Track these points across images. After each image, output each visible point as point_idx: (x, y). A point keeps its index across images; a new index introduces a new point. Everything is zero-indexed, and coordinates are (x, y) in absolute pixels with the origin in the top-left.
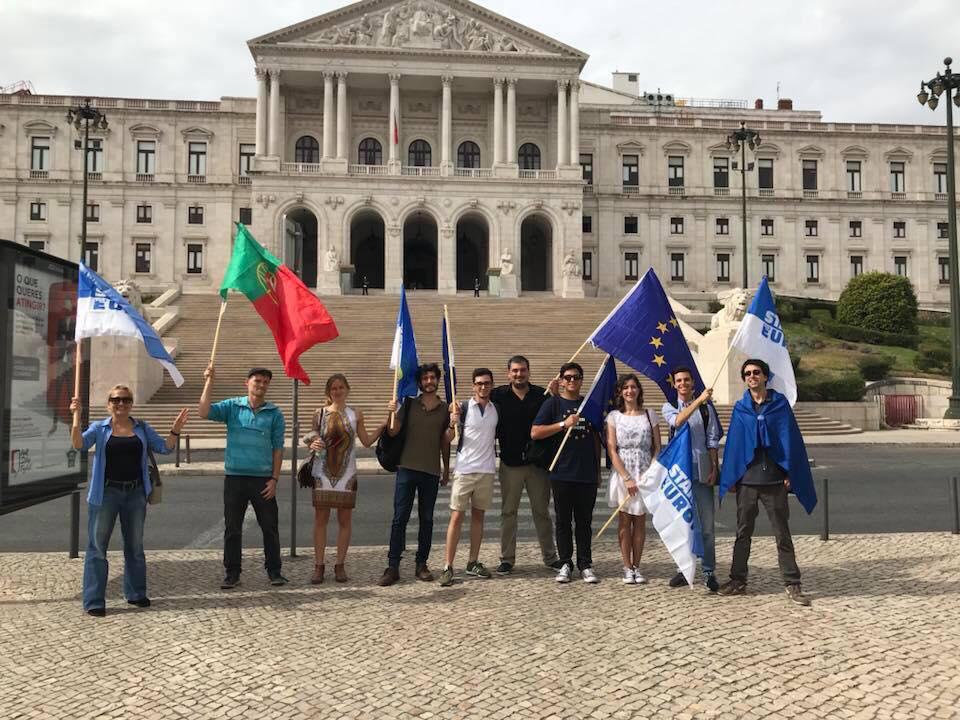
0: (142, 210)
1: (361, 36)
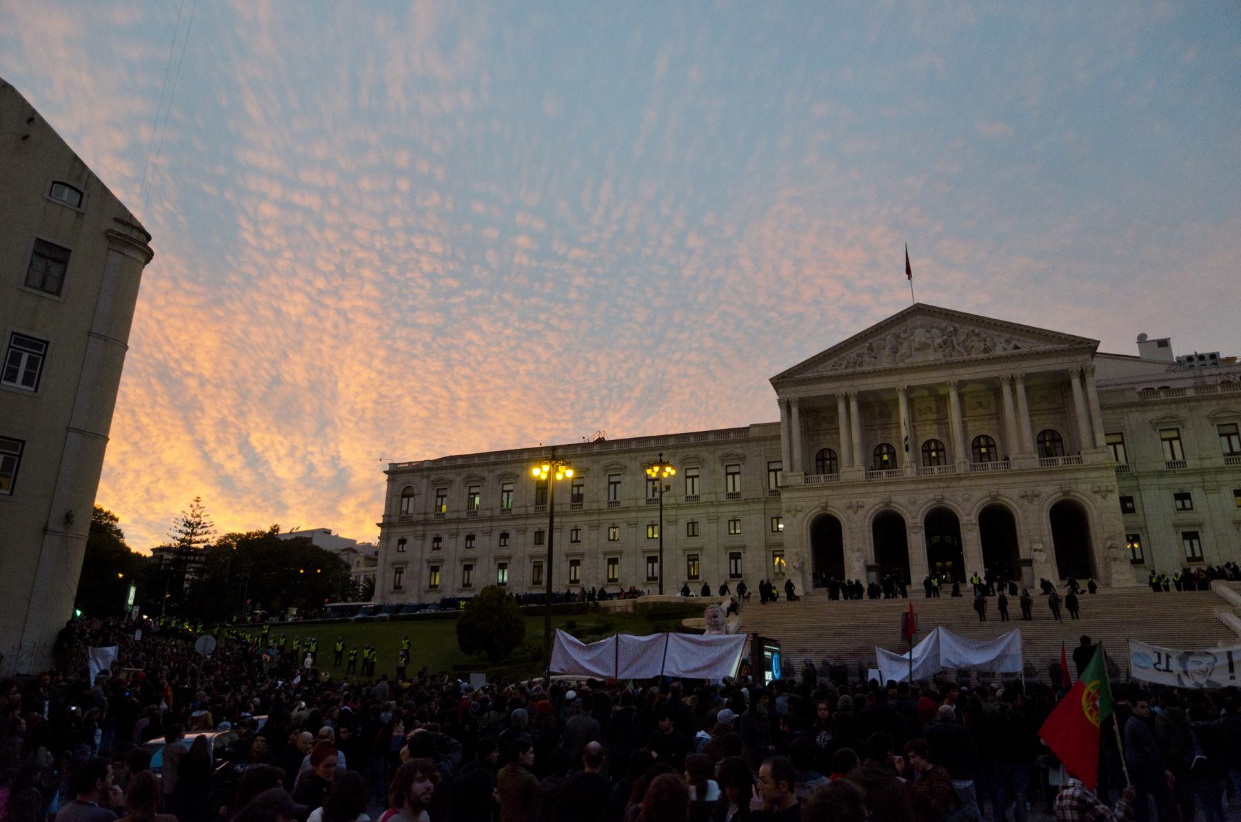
1: (866, 359)
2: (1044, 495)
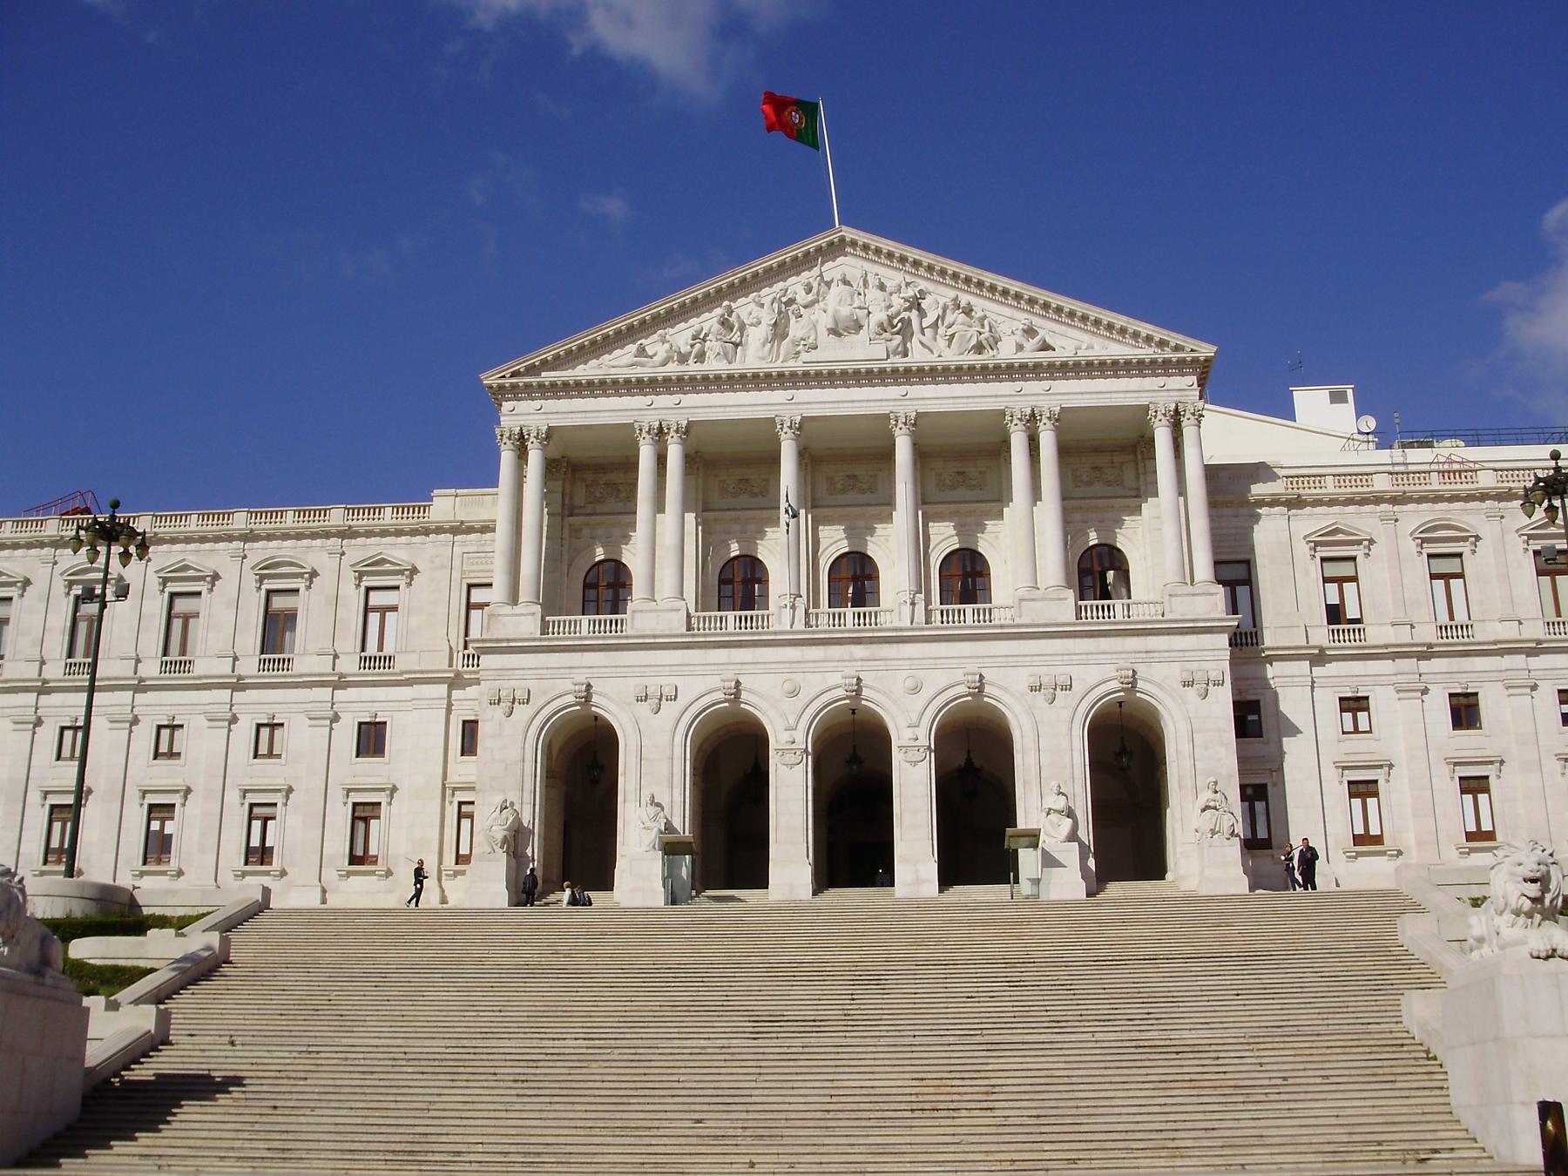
0: (265, 732)
2: (1078, 688)
